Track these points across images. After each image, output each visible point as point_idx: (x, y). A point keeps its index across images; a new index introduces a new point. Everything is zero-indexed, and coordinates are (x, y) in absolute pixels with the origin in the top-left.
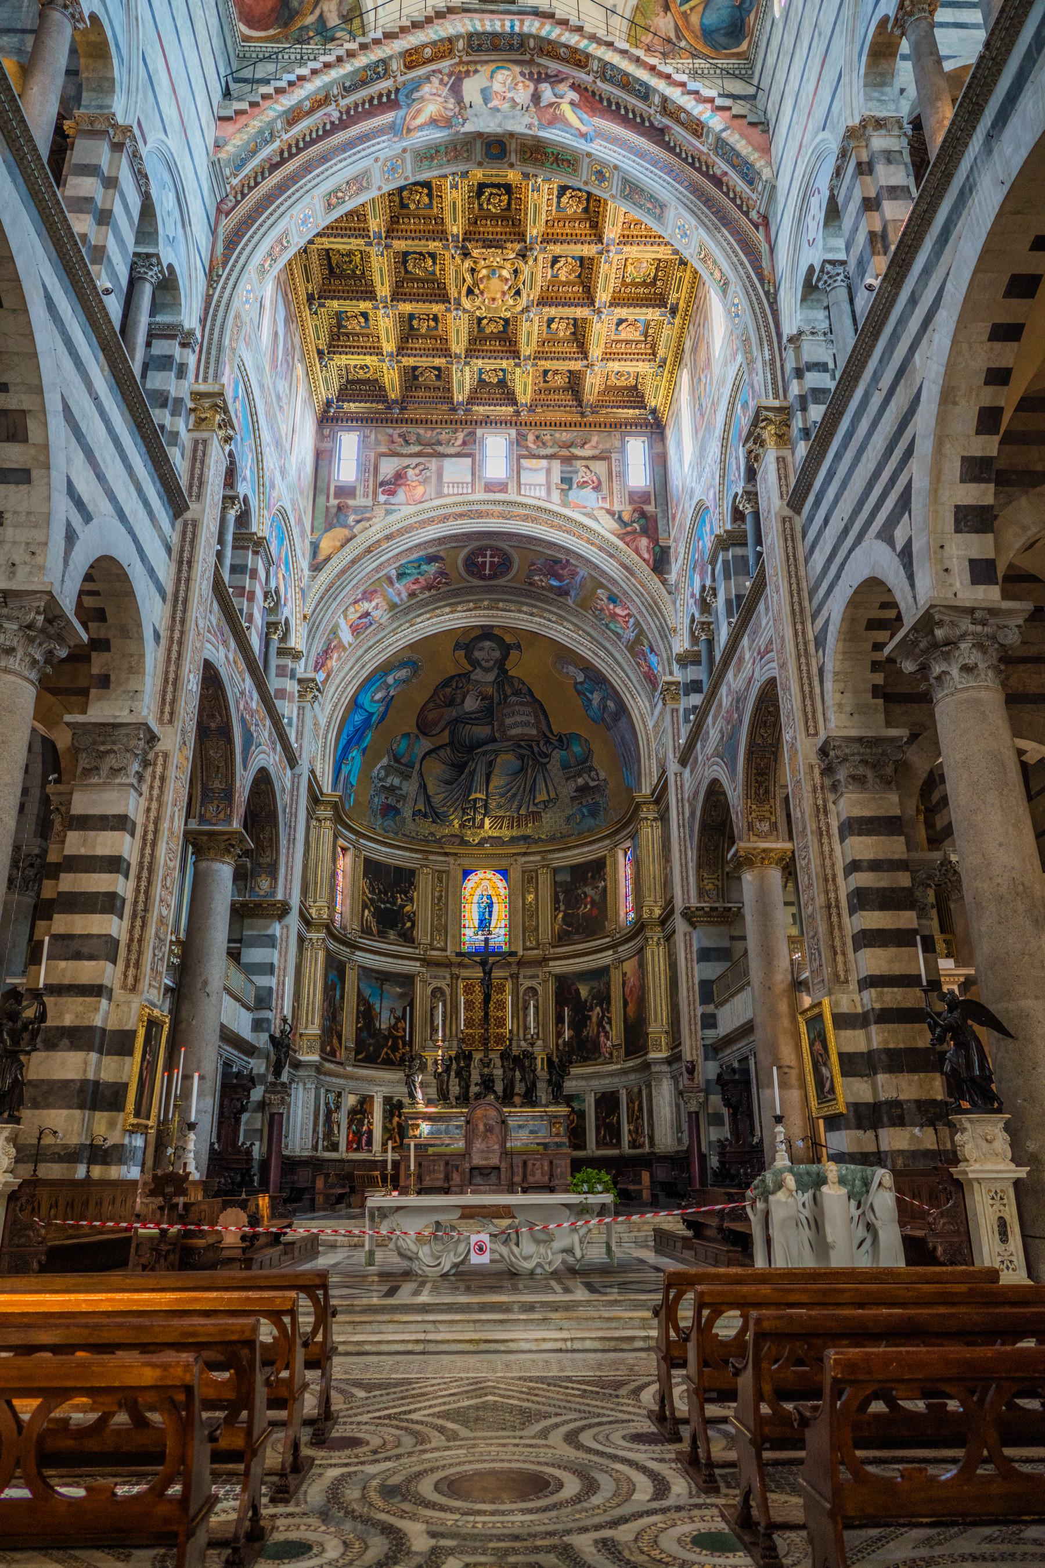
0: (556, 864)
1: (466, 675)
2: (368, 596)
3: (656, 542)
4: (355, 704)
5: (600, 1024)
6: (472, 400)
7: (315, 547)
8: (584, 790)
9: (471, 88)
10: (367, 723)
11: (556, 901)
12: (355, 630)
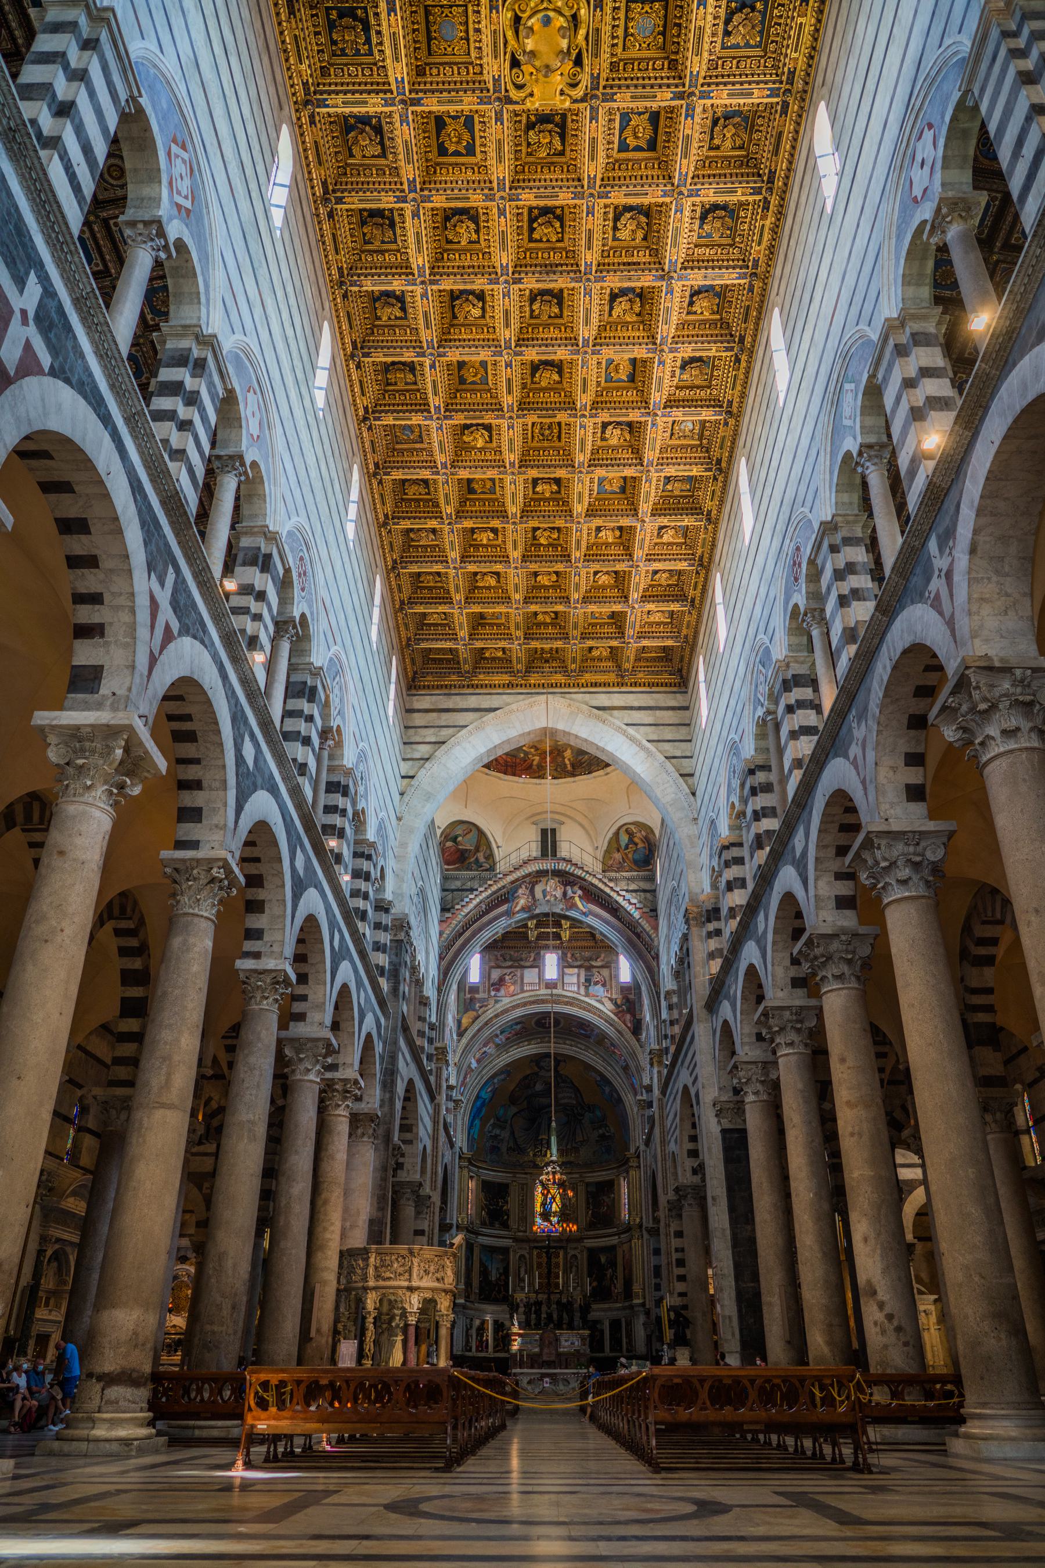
0: (587, 1180)
1: (536, 1074)
2: (485, 1045)
3: (634, 1015)
4: (478, 1097)
5: (611, 1279)
6: (540, 937)
7: (459, 1023)
8: (603, 1137)
9: (538, 889)
10: (483, 1104)
11: (588, 1203)
12: (478, 1061)
